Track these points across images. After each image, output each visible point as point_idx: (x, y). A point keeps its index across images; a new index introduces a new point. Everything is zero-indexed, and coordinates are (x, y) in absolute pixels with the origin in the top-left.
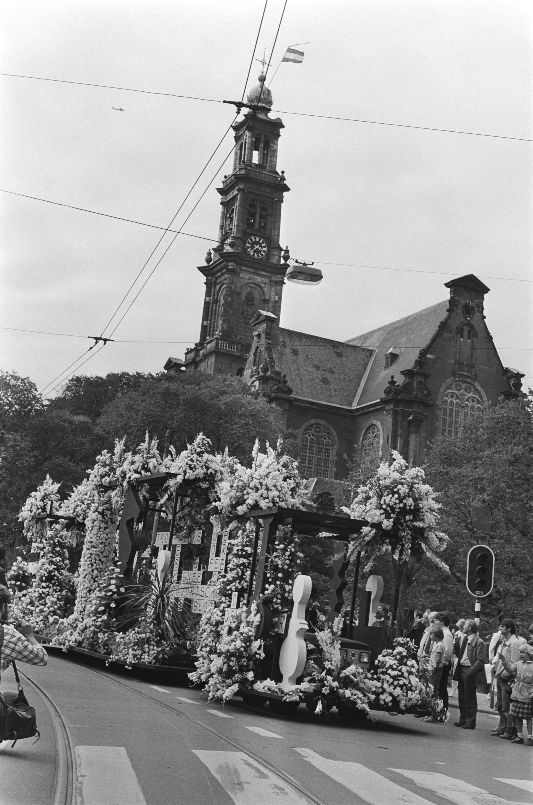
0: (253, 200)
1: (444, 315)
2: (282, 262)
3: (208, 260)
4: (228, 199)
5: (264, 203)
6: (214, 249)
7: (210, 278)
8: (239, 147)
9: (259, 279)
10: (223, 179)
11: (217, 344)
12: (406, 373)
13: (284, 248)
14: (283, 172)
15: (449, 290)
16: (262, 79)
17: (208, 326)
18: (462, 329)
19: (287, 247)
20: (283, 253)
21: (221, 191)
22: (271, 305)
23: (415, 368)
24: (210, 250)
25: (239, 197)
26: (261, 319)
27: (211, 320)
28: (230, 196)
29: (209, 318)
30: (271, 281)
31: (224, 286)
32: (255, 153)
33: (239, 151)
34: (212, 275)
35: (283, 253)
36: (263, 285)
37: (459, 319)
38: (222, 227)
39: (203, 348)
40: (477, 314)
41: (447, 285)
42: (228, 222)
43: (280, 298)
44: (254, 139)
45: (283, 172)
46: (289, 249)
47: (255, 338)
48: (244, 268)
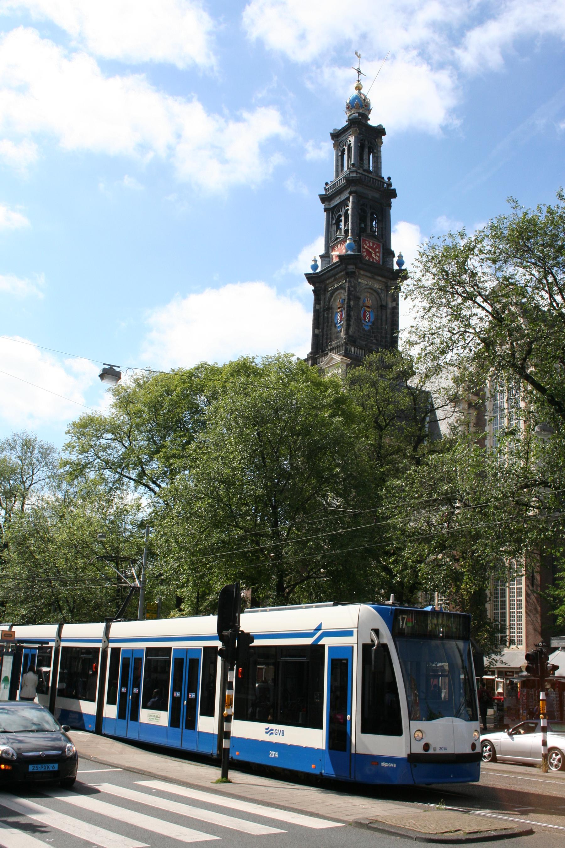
3: (315, 267)
4: (332, 206)
6: (321, 257)
10: (325, 186)
13: (397, 254)
14: (389, 178)
16: (359, 88)
17: (321, 334)
19: (400, 253)
20: (395, 260)
22: (389, 311)
27: (323, 329)
28: (336, 201)
29: (321, 326)
33: (340, 158)
36: (380, 291)
42: (334, 228)
43: (397, 304)
44: (359, 144)
46: (402, 254)
48: (362, 272)
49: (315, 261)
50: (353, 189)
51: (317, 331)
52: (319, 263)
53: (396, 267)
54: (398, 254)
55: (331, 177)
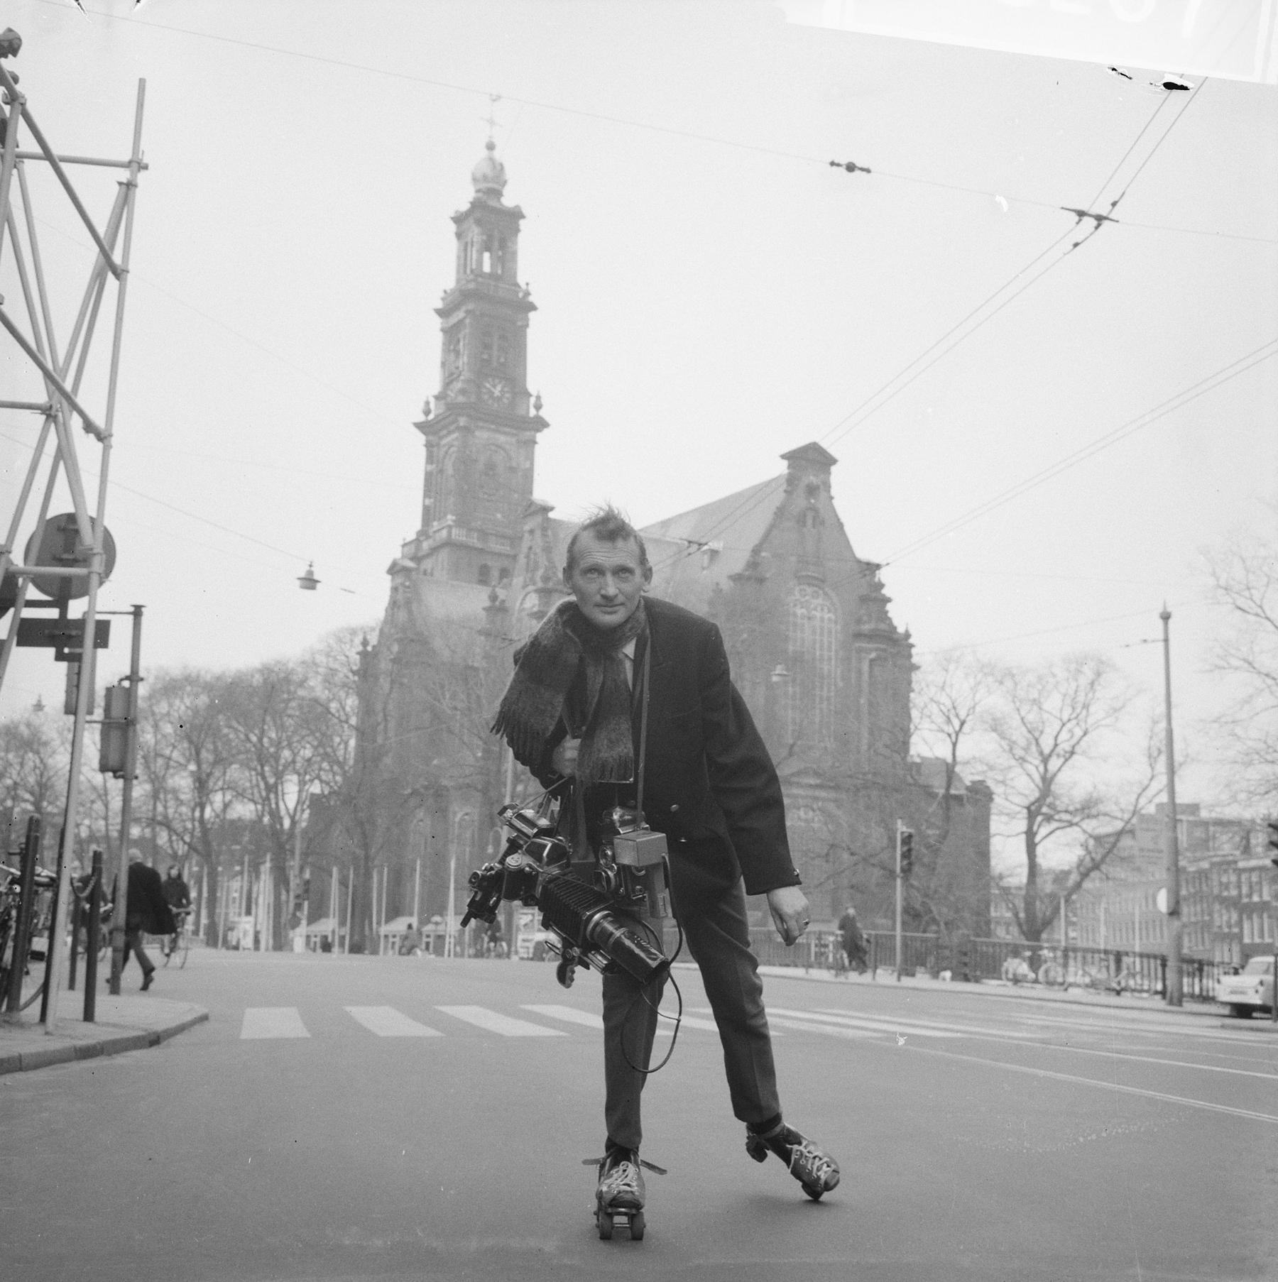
1: (778, 497)
2: (533, 412)
3: (427, 412)
7: (431, 438)
9: (502, 439)
11: (450, 533)
12: (736, 578)
14: (527, 284)
15: (785, 463)
16: (491, 147)
17: (433, 506)
18: (805, 516)
19: (539, 392)
20: (532, 400)
21: (441, 313)
23: (746, 570)
24: (428, 397)
25: (467, 321)
26: (533, 509)
28: (454, 319)
31: (453, 449)
32: (487, 255)
34: (435, 433)
36: (507, 447)
37: (800, 502)
38: (443, 364)
39: (428, 537)
40: (823, 494)
41: (783, 457)
42: (452, 356)
43: (532, 464)
44: (484, 237)
45: (527, 284)
46: (541, 395)
47: (526, 535)
49: (427, 403)
50: (471, 306)
51: (428, 502)
53: (533, 412)
55: (450, 282)
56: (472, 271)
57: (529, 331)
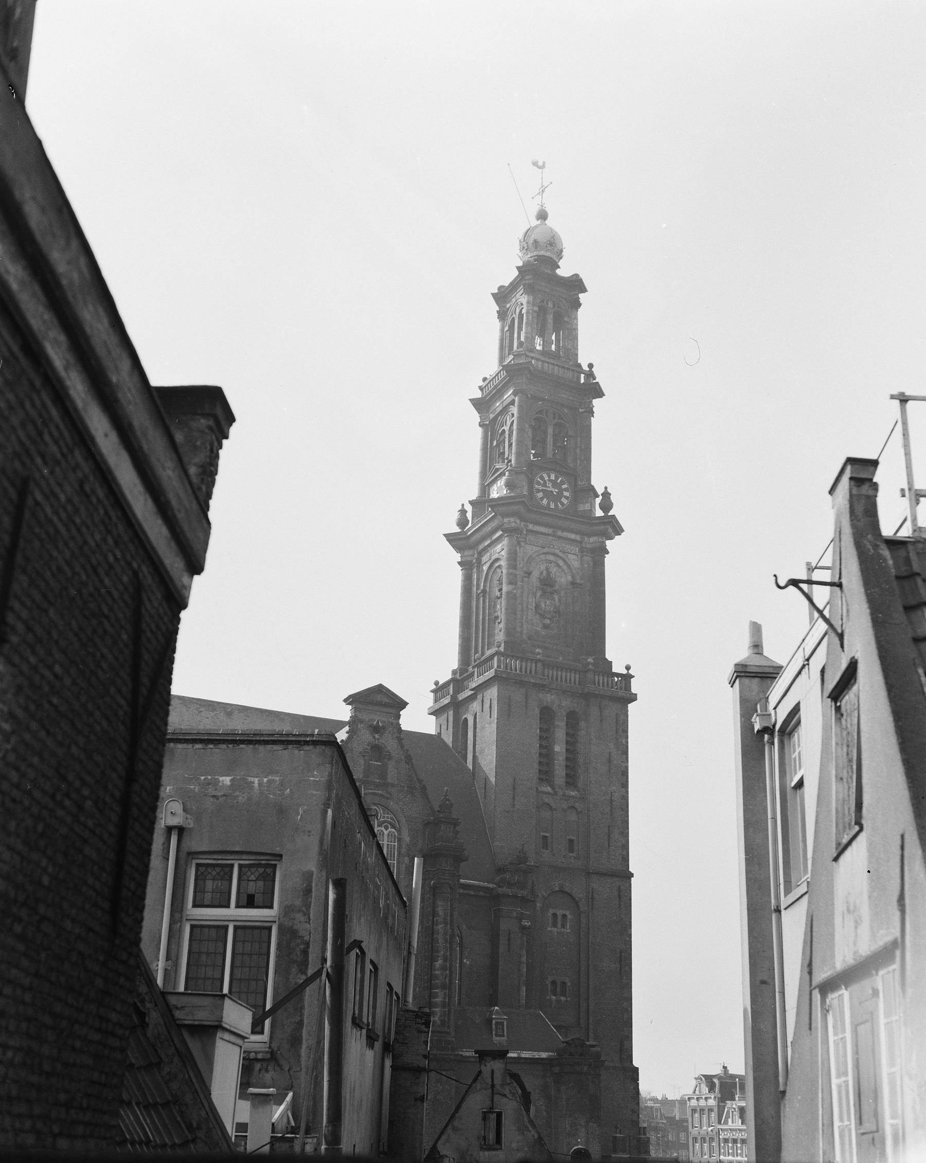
0: (540, 412)
3: (462, 522)
5: (560, 418)
6: (471, 503)
7: (466, 553)
8: (506, 328)
13: (600, 491)
14: (591, 366)
16: (543, 216)
19: (606, 488)
24: (463, 505)
30: (582, 550)
35: (598, 500)
44: (536, 309)
45: (591, 366)
46: (609, 490)
52: (469, 516)
54: (603, 490)
56: (521, 344)
57: (594, 421)
